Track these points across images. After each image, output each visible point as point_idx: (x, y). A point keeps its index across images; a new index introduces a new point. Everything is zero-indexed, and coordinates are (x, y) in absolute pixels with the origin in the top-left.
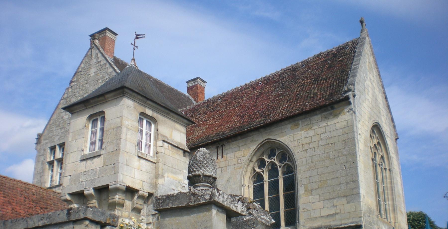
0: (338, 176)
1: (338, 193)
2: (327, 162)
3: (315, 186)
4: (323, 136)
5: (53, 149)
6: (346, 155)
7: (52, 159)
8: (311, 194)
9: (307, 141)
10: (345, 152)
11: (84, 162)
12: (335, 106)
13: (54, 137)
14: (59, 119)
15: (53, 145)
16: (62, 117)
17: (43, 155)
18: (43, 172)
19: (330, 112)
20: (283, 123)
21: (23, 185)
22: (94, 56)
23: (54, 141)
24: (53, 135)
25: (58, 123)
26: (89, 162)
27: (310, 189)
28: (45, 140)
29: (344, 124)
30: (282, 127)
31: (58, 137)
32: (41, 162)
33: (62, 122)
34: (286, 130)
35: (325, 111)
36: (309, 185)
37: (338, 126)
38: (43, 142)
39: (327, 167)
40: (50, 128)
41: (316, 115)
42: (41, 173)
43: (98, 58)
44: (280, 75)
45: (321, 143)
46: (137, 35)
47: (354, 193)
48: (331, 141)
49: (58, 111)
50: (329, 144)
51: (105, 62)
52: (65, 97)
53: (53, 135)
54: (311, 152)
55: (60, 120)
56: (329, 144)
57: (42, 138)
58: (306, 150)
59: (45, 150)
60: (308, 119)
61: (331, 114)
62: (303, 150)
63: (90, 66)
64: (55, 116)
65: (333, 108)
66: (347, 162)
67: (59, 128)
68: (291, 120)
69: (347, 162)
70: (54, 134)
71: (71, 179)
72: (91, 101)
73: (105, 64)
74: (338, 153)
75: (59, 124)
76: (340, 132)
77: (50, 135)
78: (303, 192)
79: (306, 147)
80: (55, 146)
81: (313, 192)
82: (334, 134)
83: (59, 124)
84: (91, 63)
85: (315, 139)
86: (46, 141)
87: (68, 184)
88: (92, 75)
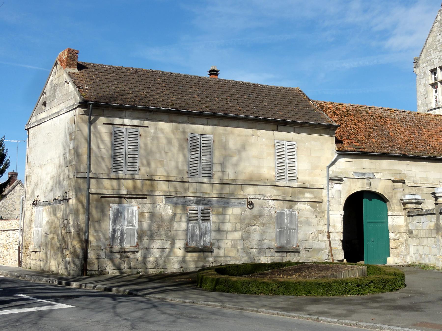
5: (434, 71)
7: (433, 81)
13: (433, 60)
14: (436, 42)
15: (433, 67)
16: (439, 40)
17: (424, 78)
18: (427, 93)
21: (433, 117)
23: (434, 64)
24: (432, 58)
25: (435, 46)
28: (423, 63)
31: (437, 60)
32: (423, 85)
33: (439, 45)
38: (422, 65)
40: (427, 51)
42: (425, 95)
49: (432, 34)
52: (438, 20)
53: (432, 58)
55: (437, 43)
57: (420, 61)
59: (425, 73)
64: (430, 40)
67: (437, 51)
70: (433, 57)
75: (437, 47)
77: (429, 58)
80: (436, 69)
83: (437, 47)
86: (425, 64)
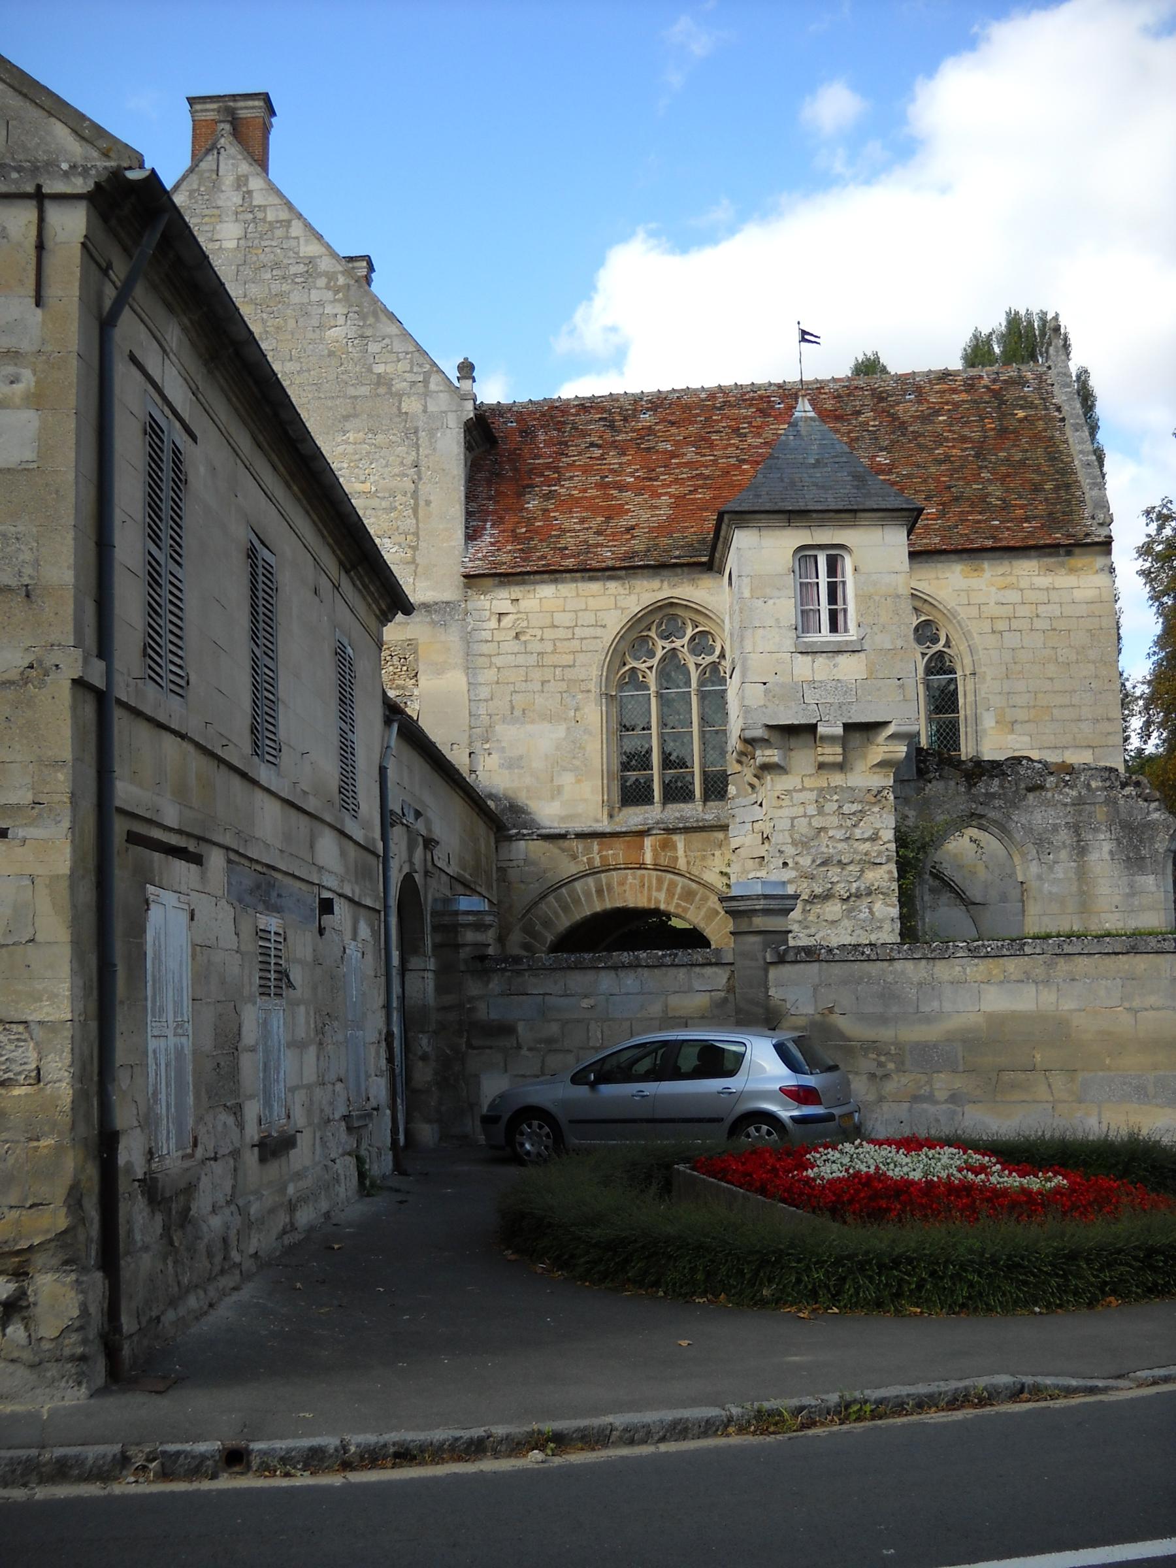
0: (1075, 701)
1: (1074, 739)
2: (1051, 669)
3: (1021, 715)
4: (1042, 609)
6: (1094, 662)
8: (1012, 731)
9: (1006, 611)
10: (1093, 654)
11: (809, 658)
12: (1077, 550)
19: (1060, 559)
20: (943, 558)
22: (228, 180)
26: (821, 660)
27: (1008, 719)
29: (1090, 594)
30: (939, 565)
34: (948, 575)
35: (1050, 555)
36: (1007, 710)
37: (1078, 595)
39: (1051, 679)
41: (1028, 557)
43: (250, 192)
44: (838, 397)
45: (1039, 624)
46: (804, 332)
47: (1110, 743)
48: (1061, 625)
50: (1055, 630)
51: (284, 215)
54: (1011, 640)
56: (1055, 630)
58: (1001, 633)
60: (1006, 562)
61: (1062, 565)
62: (993, 632)
63: (216, 212)
65: (1069, 553)
66: (1096, 677)
68: (965, 556)
69: (1096, 677)
71: (766, 692)
72: (814, 515)
73: (288, 224)
74: (1077, 653)
76: (1083, 610)
78: (993, 724)
79: (1001, 625)
81: (1017, 727)
82: (1068, 610)
84: (220, 203)
85: (1023, 611)
87: (762, 703)
88: (231, 244)
